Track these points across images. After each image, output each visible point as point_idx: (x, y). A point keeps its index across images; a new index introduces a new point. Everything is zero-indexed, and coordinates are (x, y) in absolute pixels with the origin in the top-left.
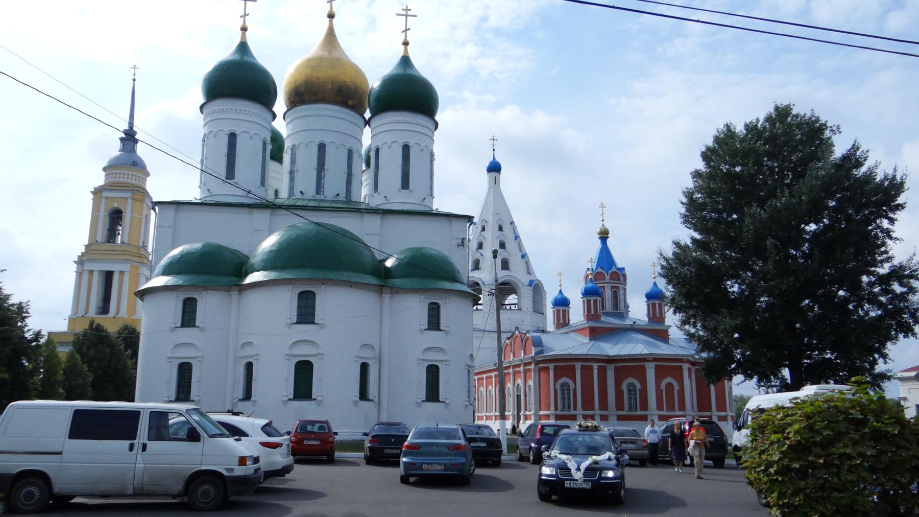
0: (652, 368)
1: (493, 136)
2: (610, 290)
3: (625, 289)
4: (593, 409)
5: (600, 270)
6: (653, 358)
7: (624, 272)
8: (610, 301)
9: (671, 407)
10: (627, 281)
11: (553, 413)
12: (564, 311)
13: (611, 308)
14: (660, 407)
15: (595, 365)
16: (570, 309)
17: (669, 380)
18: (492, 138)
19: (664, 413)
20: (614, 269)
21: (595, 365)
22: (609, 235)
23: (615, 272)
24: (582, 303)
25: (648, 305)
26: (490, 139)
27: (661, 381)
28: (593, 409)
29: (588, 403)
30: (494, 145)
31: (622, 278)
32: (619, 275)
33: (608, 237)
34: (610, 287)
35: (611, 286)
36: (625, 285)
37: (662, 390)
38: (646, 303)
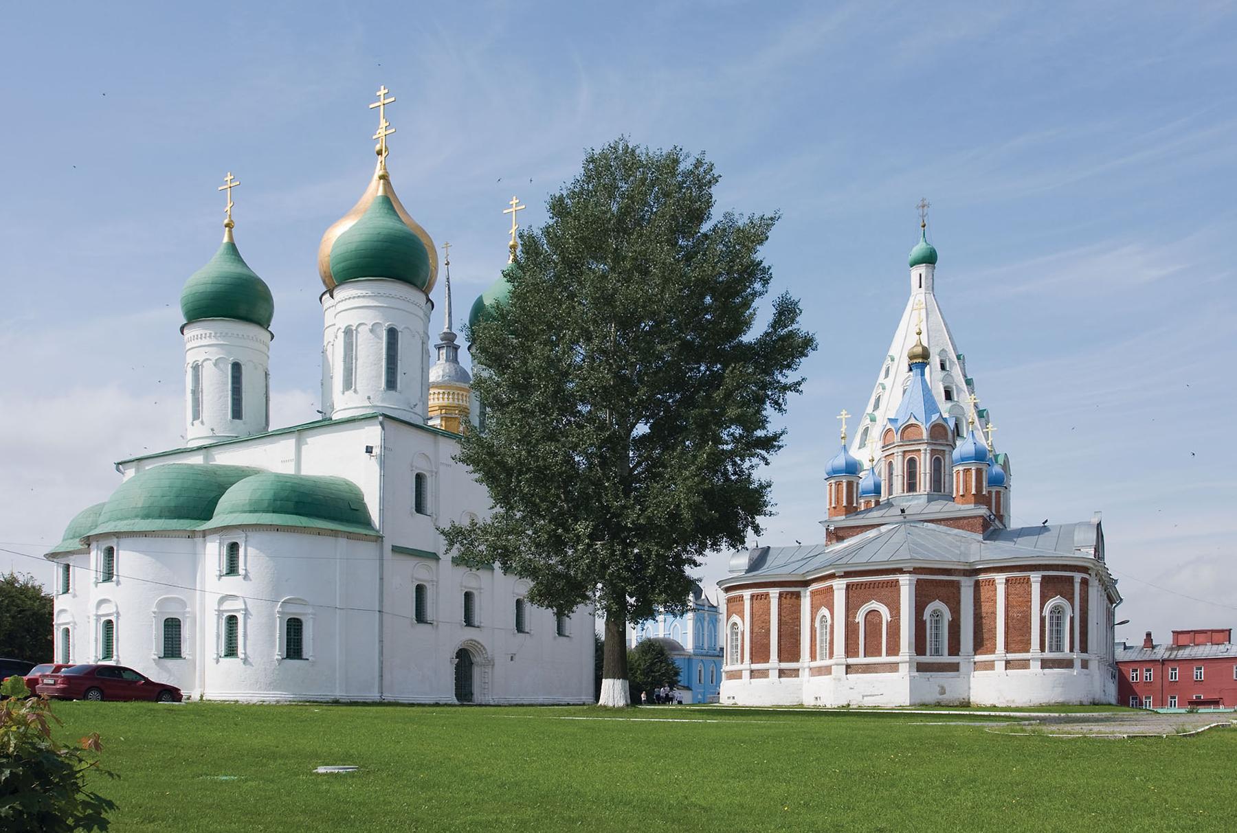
0: (842, 589)
1: (923, 200)
4: (766, 659)
6: (845, 572)
9: (873, 649)
11: (748, 667)
14: (850, 650)
15: (774, 593)
17: (874, 605)
18: (921, 204)
19: (861, 660)
21: (774, 593)
26: (918, 207)
27: (858, 608)
28: (766, 659)
29: (759, 652)
30: (923, 216)
37: (925, 622)
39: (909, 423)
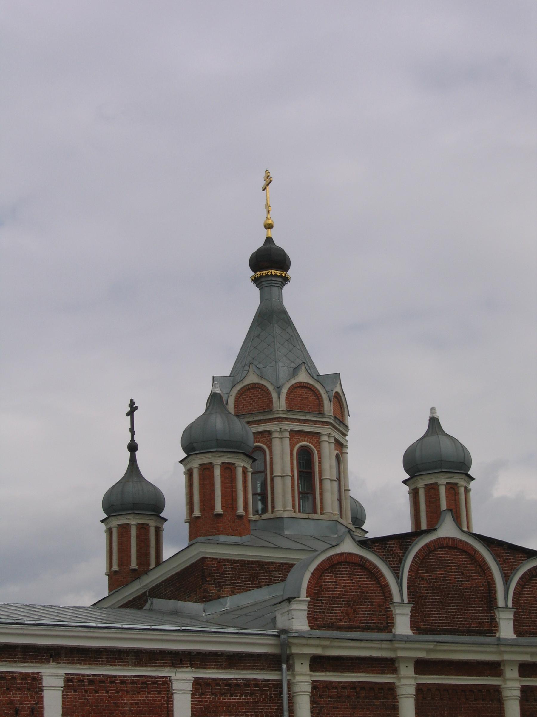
2: (287, 442)
3: (340, 446)
5: (252, 379)
7: (338, 389)
8: (289, 481)
10: (351, 422)
12: (143, 529)
13: (290, 507)
16: (166, 526)
20: (302, 377)
22: (290, 273)
23: (302, 386)
24: (182, 479)
25: (414, 494)
31: (328, 407)
32: (318, 396)
33: (286, 280)
34: (287, 435)
35: (292, 432)
36: (345, 435)
38: (406, 488)
39: (247, 382)
